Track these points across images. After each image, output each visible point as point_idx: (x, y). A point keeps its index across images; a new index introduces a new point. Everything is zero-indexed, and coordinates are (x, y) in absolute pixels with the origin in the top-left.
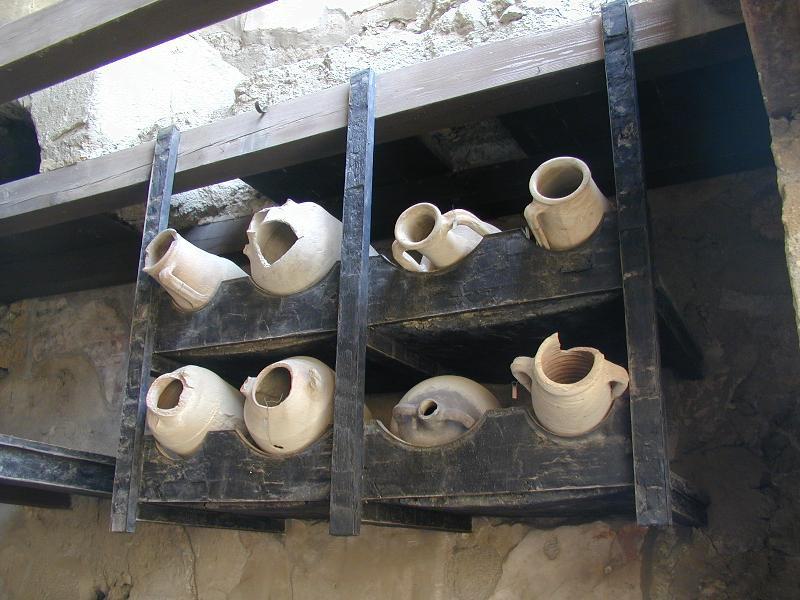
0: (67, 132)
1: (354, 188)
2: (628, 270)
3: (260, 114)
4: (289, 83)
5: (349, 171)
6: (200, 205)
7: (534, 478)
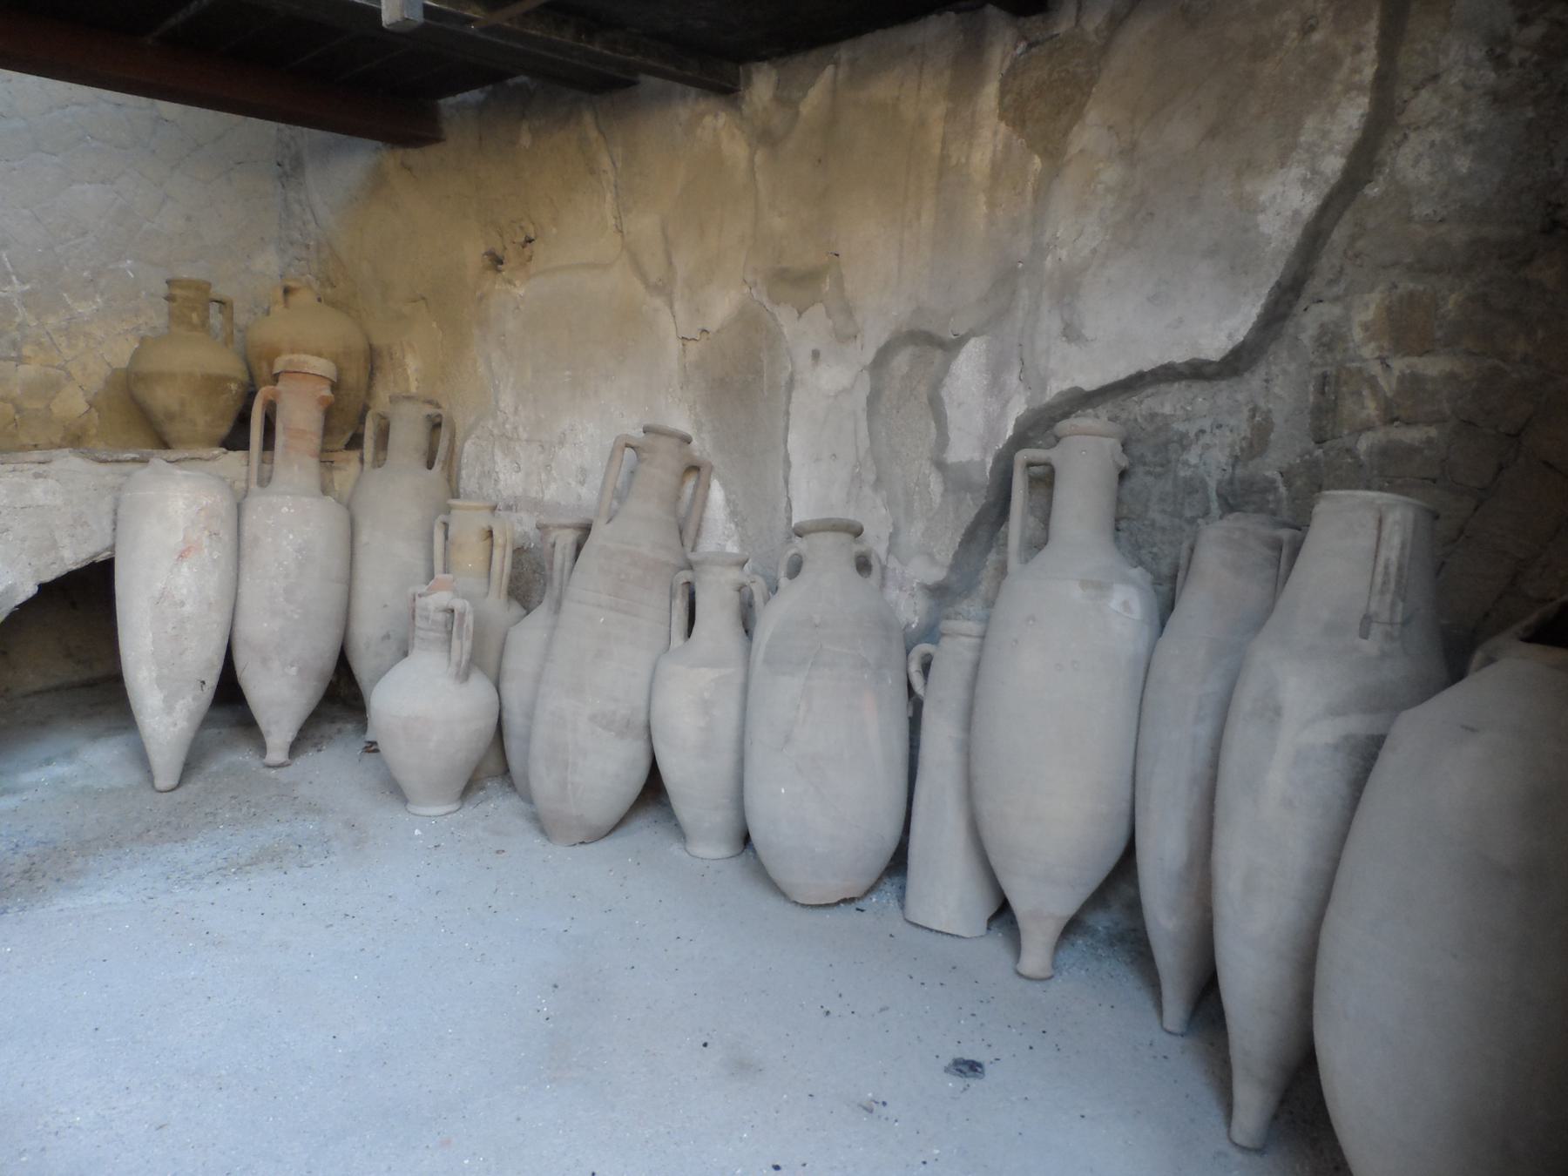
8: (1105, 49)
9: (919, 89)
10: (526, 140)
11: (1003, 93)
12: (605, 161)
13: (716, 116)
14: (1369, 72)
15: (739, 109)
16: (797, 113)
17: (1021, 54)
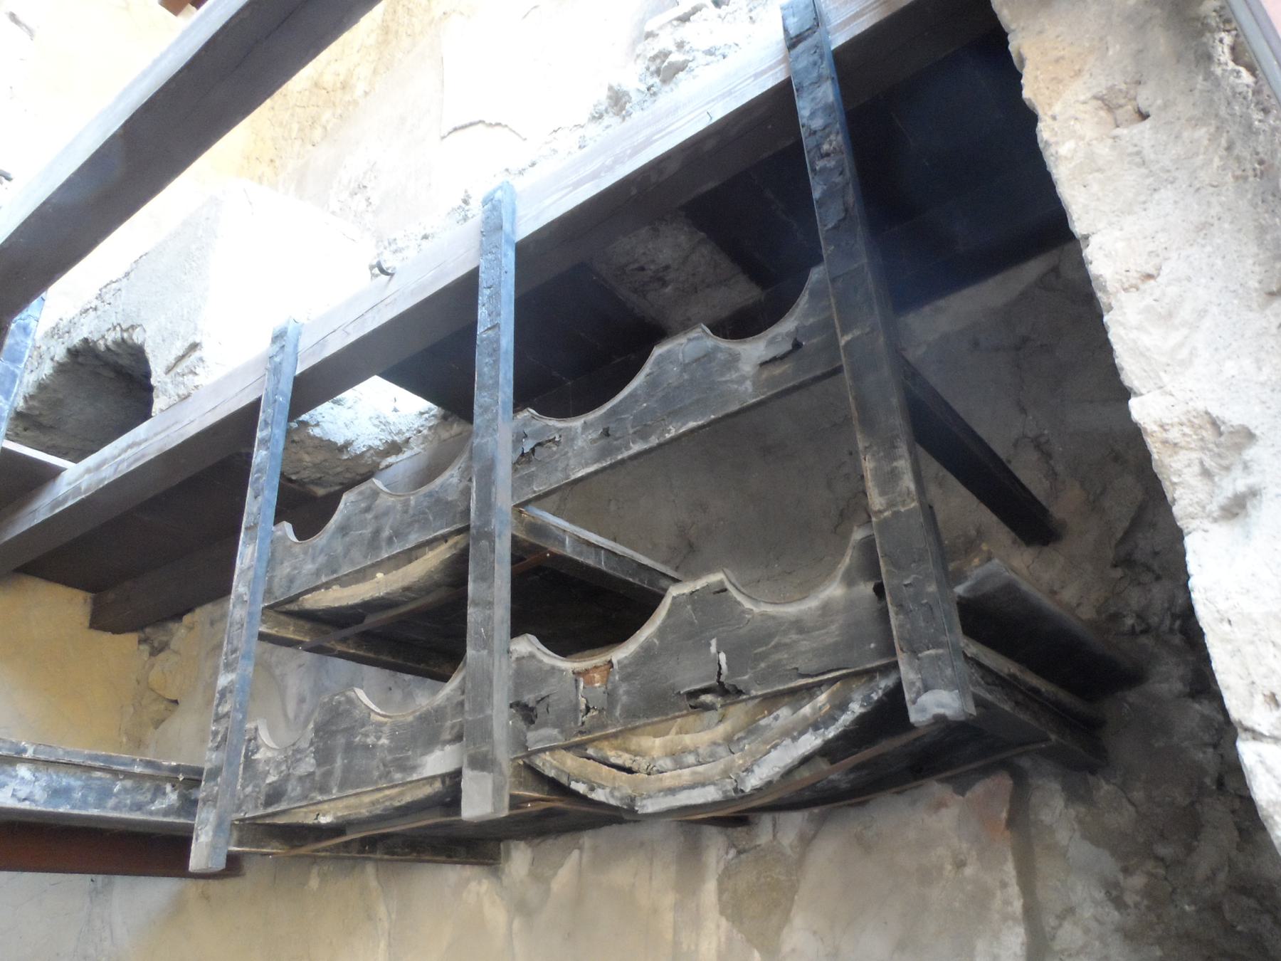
0: (180, 359)
1: (489, 329)
2: (844, 332)
3: (388, 277)
4: (425, 237)
5: (482, 312)
6: (377, 443)
7: (746, 677)
8: (801, 861)
9: (651, 878)
10: (314, 883)
11: (721, 891)
12: (382, 911)
13: (480, 883)
14: (1018, 905)
15: (499, 878)
16: (548, 890)
17: (732, 859)
